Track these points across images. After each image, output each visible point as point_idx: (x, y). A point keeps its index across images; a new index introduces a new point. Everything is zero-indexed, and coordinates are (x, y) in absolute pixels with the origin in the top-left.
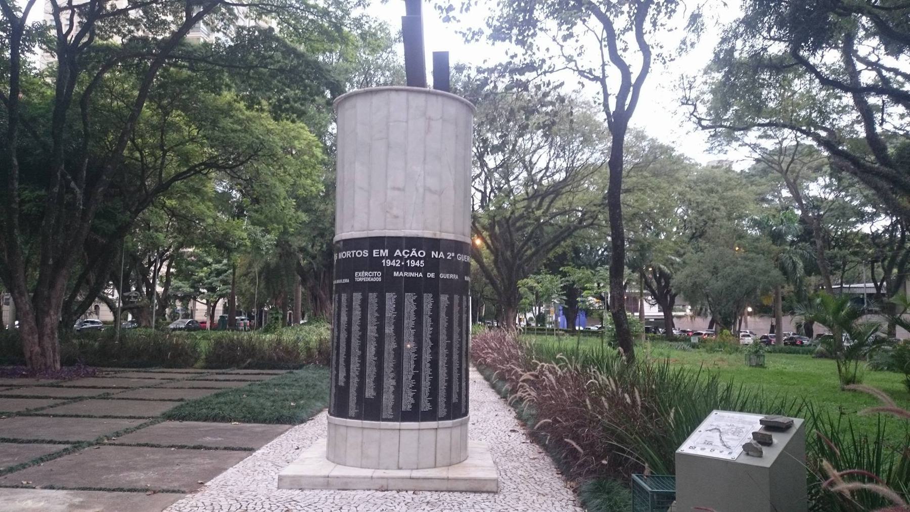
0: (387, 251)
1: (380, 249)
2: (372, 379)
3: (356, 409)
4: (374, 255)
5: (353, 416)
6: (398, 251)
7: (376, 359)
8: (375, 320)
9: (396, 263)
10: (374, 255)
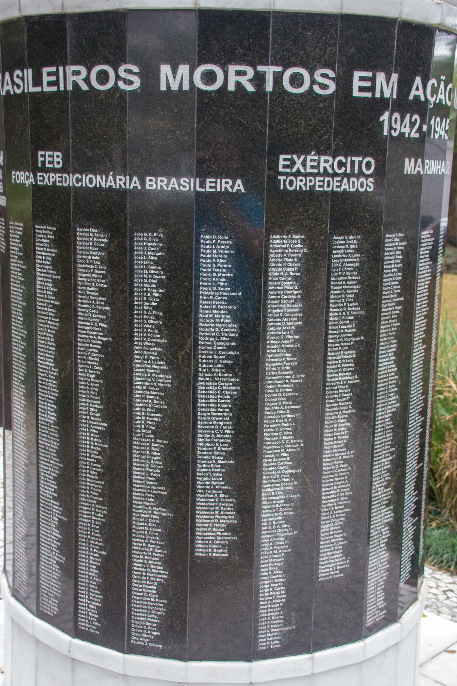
0: (395, 77)
1: (374, 68)
2: (339, 522)
3: (287, 622)
4: (356, 93)
5: (276, 644)
6: (418, 80)
7: (349, 455)
8: (351, 328)
9: (412, 125)
10: (356, 93)
